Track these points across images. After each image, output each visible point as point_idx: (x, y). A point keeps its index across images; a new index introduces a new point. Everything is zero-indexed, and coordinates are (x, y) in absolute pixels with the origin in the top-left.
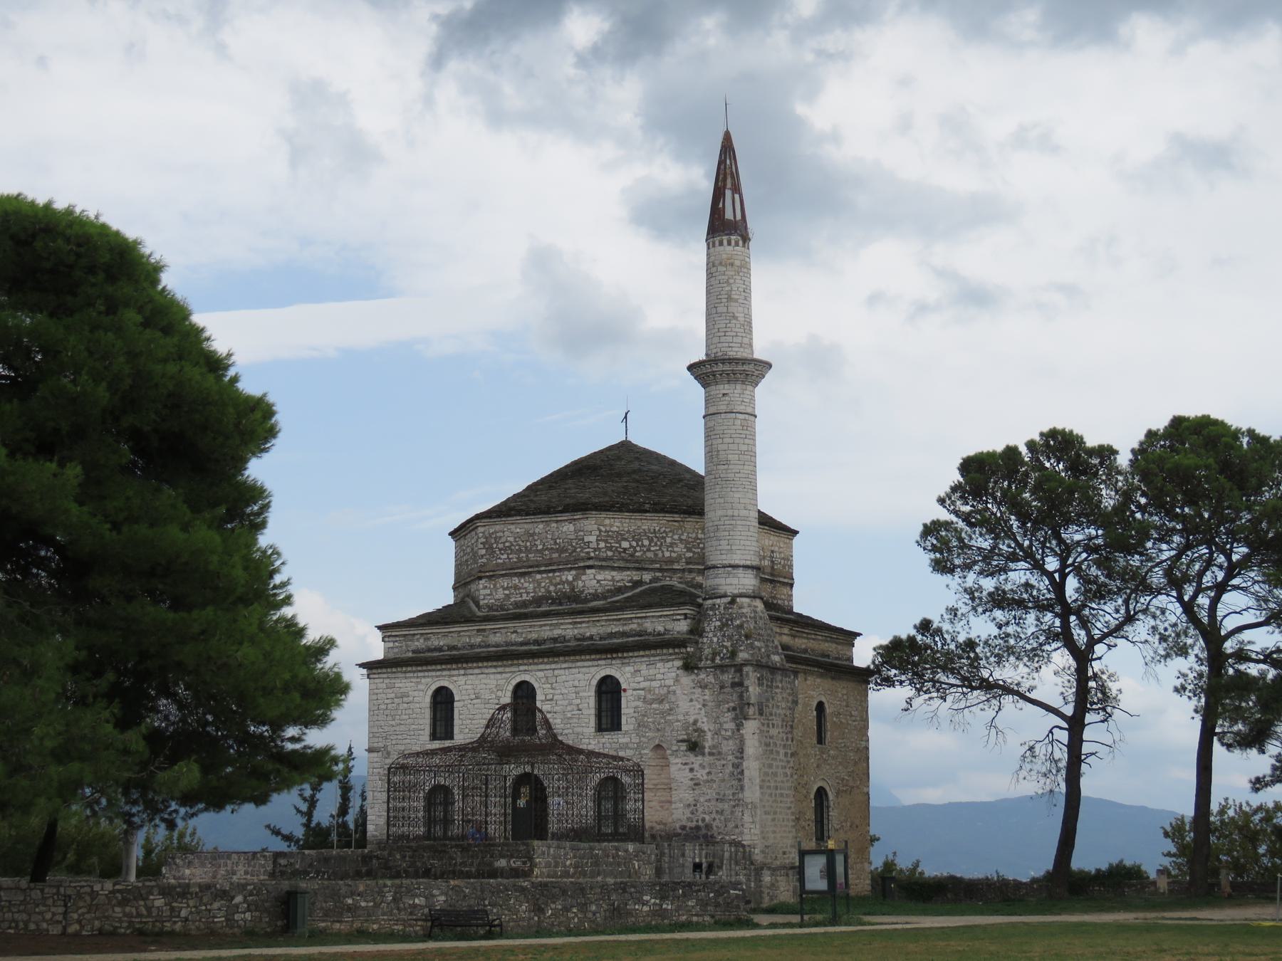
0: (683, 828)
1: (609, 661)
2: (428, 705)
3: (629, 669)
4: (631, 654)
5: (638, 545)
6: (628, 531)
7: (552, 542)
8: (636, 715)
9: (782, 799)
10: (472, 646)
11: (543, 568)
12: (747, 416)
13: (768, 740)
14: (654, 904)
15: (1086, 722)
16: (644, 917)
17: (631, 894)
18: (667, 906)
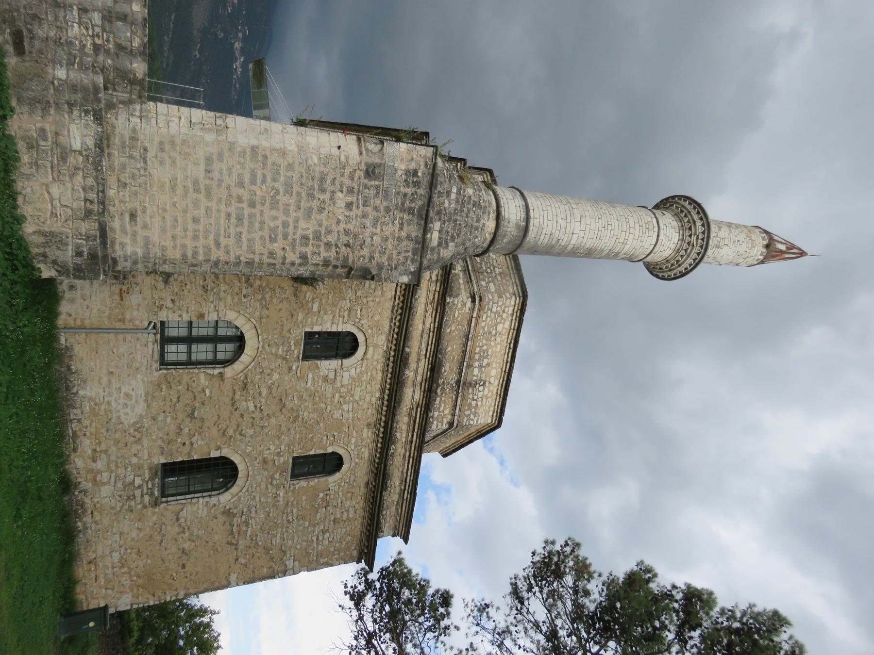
9: (233, 220)
12: (656, 229)
13: (327, 185)
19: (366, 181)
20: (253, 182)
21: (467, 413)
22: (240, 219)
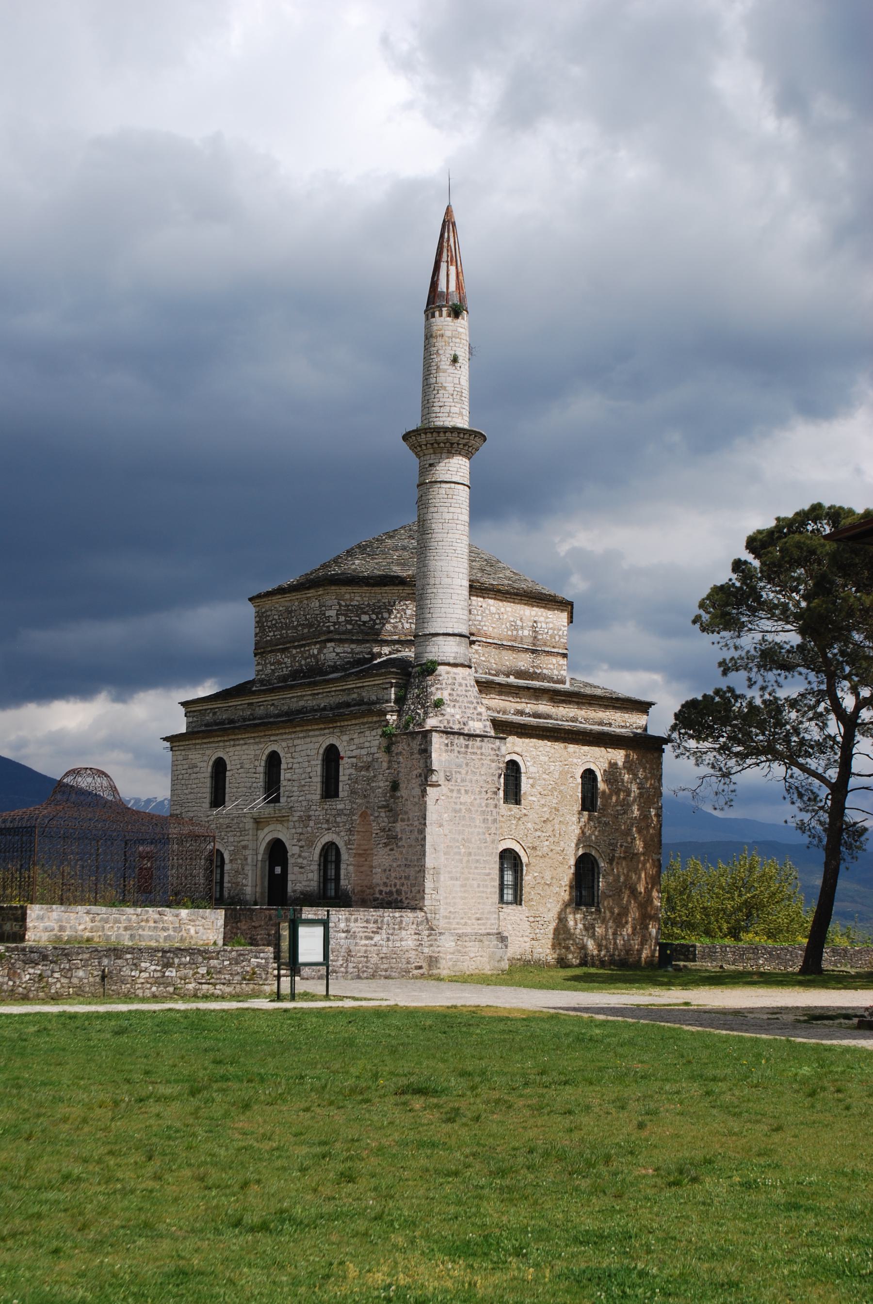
0: (381, 892)
1: (331, 730)
2: (208, 775)
3: (345, 738)
4: (346, 723)
5: (377, 618)
6: (369, 605)
7: (303, 618)
8: (349, 782)
9: (478, 865)
10: (245, 720)
11: (296, 644)
12: (453, 485)
13: (458, 807)
14: (155, 971)
15: (849, 789)
16: (142, 983)
17: (126, 960)
18: (171, 973)
19: (453, 780)
20: (459, 853)
21: (557, 638)
22: (477, 861)
